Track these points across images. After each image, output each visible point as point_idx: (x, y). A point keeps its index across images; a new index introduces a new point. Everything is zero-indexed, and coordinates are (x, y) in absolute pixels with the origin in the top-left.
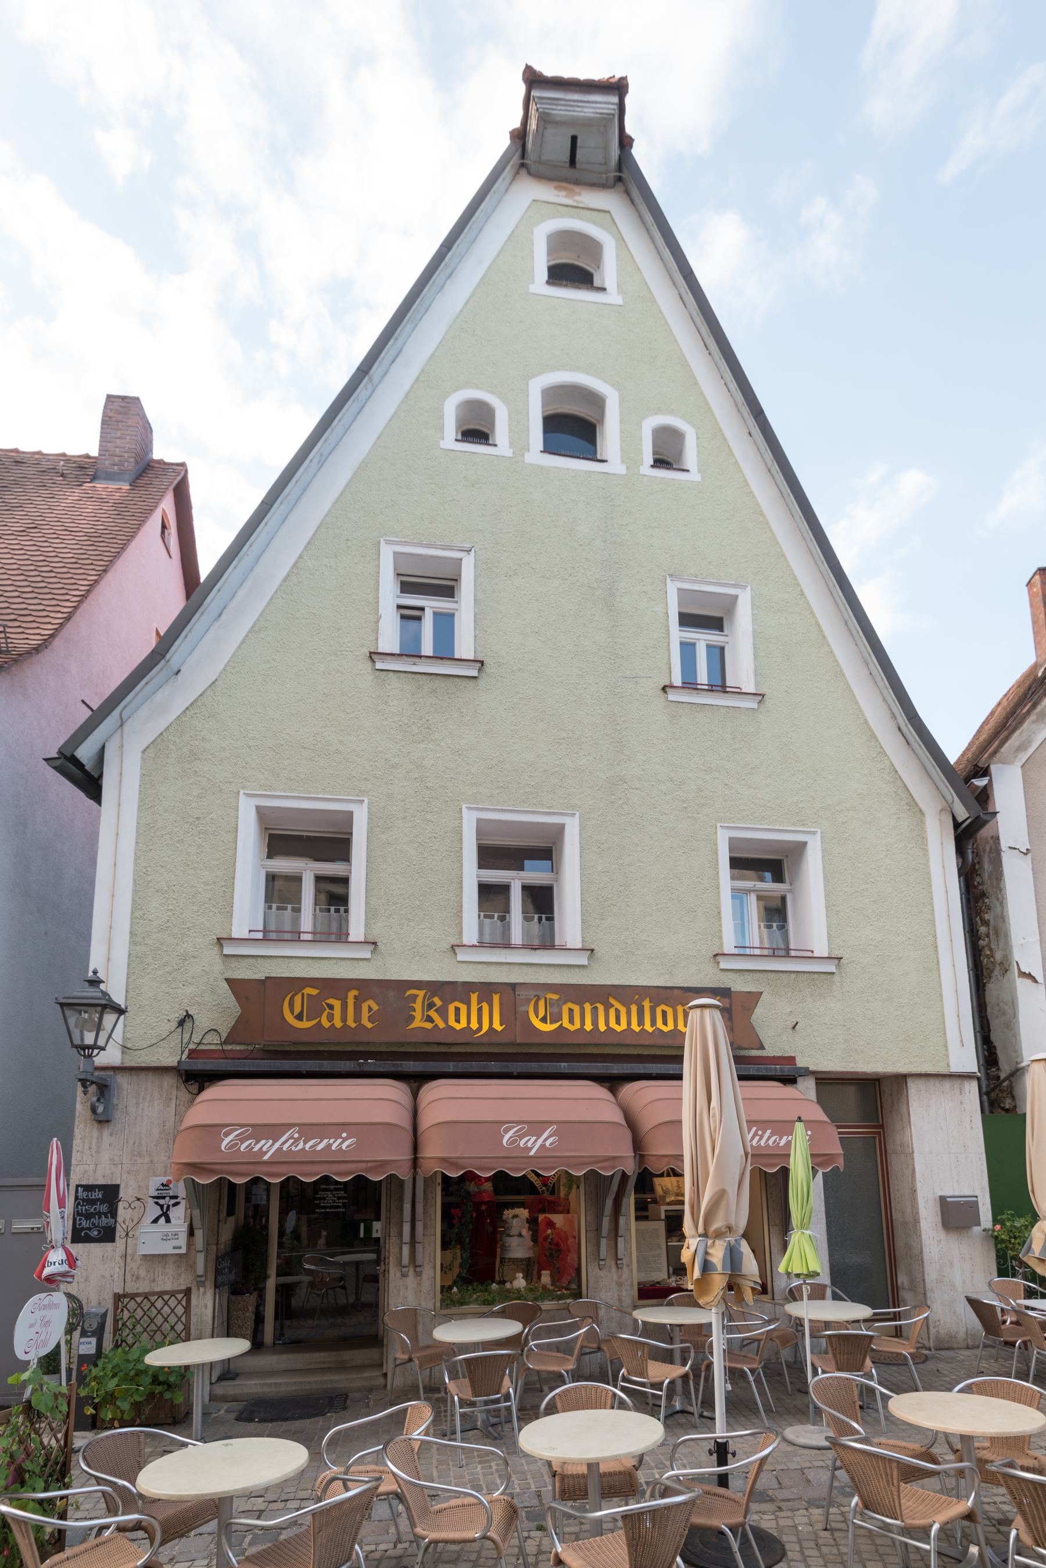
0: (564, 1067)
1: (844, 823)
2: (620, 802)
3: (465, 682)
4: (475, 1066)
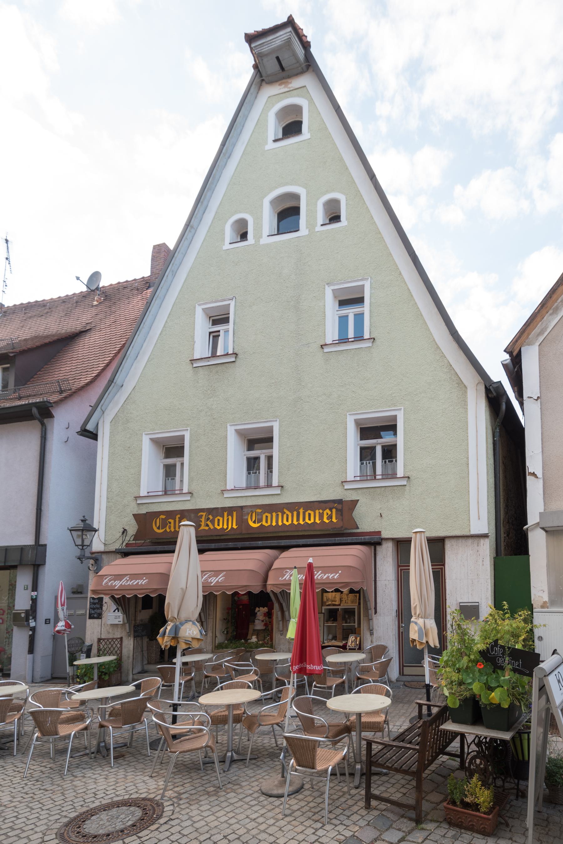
0: (260, 543)
1: (418, 401)
2: (299, 410)
3: (230, 365)
4: (223, 545)
